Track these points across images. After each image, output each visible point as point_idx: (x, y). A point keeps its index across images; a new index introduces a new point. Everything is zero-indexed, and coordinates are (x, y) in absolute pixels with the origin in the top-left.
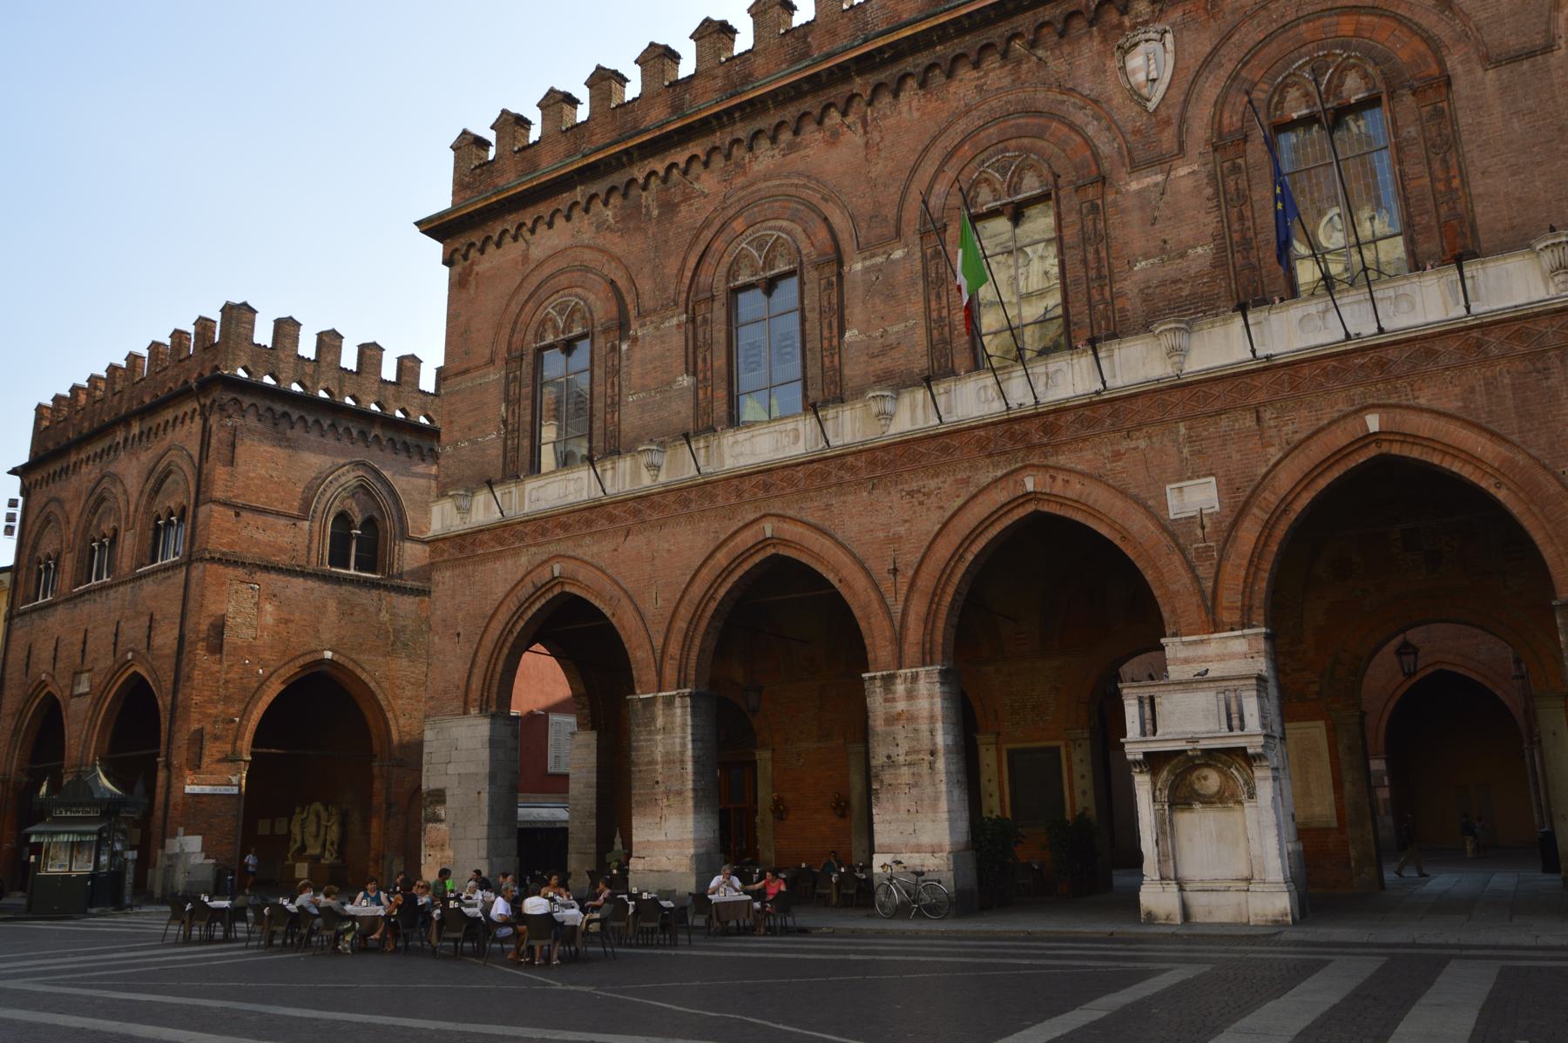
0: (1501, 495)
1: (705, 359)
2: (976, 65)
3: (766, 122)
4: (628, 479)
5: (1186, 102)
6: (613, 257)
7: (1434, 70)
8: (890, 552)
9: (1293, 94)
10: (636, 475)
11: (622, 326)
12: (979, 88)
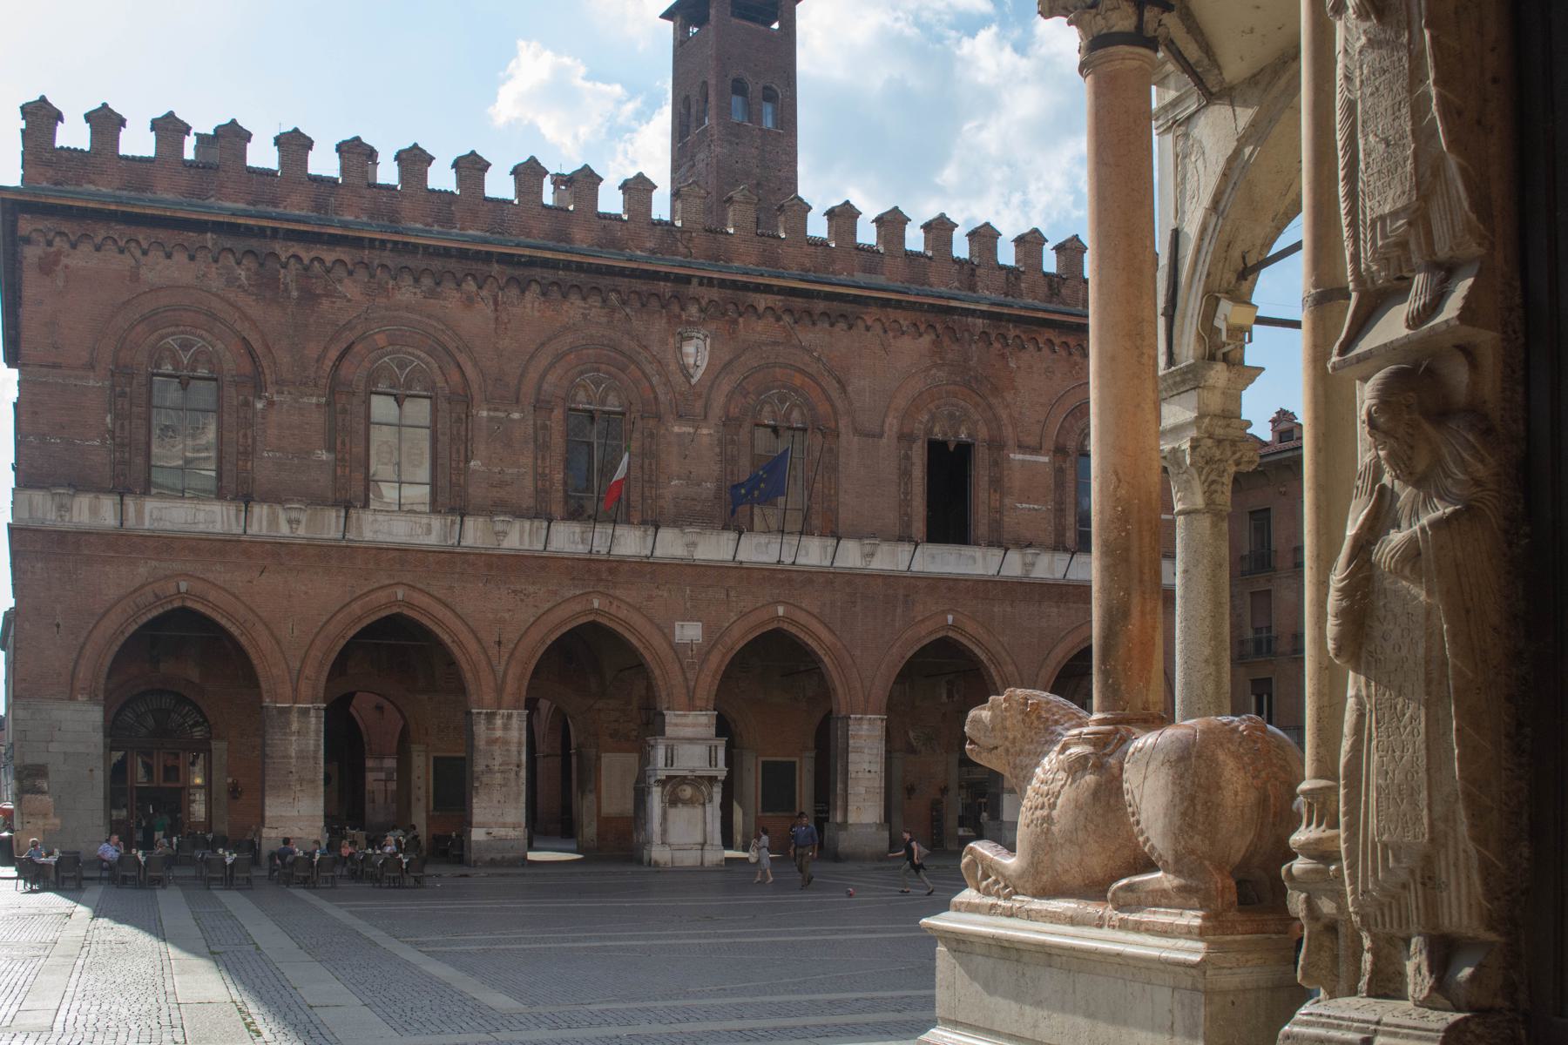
0: (826, 659)
1: (343, 443)
2: (584, 299)
3: (417, 262)
4: (265, 523)
5: (712, 387)
6: (245, 317)
7: (832, 424)
8: (494, 634)
9: (767, 408)
10: (273, 521)
11: (259, 387)
12: (585, 316)
